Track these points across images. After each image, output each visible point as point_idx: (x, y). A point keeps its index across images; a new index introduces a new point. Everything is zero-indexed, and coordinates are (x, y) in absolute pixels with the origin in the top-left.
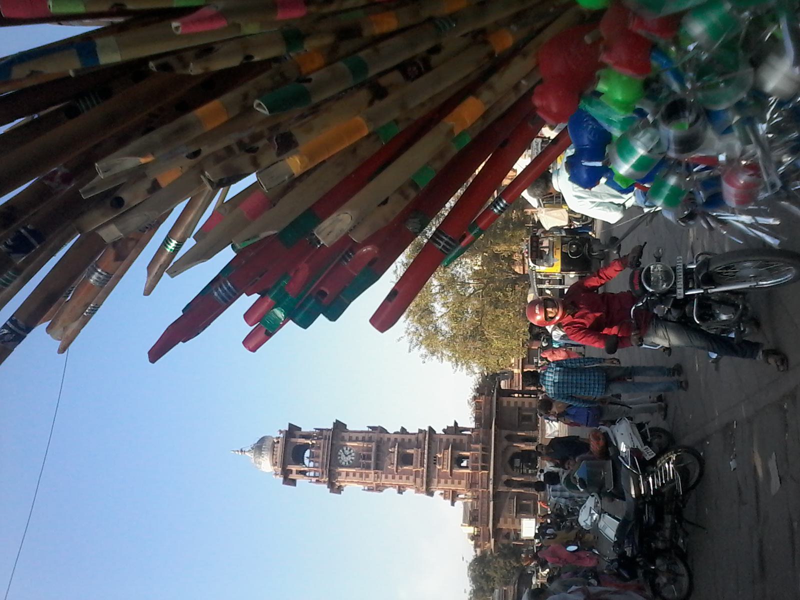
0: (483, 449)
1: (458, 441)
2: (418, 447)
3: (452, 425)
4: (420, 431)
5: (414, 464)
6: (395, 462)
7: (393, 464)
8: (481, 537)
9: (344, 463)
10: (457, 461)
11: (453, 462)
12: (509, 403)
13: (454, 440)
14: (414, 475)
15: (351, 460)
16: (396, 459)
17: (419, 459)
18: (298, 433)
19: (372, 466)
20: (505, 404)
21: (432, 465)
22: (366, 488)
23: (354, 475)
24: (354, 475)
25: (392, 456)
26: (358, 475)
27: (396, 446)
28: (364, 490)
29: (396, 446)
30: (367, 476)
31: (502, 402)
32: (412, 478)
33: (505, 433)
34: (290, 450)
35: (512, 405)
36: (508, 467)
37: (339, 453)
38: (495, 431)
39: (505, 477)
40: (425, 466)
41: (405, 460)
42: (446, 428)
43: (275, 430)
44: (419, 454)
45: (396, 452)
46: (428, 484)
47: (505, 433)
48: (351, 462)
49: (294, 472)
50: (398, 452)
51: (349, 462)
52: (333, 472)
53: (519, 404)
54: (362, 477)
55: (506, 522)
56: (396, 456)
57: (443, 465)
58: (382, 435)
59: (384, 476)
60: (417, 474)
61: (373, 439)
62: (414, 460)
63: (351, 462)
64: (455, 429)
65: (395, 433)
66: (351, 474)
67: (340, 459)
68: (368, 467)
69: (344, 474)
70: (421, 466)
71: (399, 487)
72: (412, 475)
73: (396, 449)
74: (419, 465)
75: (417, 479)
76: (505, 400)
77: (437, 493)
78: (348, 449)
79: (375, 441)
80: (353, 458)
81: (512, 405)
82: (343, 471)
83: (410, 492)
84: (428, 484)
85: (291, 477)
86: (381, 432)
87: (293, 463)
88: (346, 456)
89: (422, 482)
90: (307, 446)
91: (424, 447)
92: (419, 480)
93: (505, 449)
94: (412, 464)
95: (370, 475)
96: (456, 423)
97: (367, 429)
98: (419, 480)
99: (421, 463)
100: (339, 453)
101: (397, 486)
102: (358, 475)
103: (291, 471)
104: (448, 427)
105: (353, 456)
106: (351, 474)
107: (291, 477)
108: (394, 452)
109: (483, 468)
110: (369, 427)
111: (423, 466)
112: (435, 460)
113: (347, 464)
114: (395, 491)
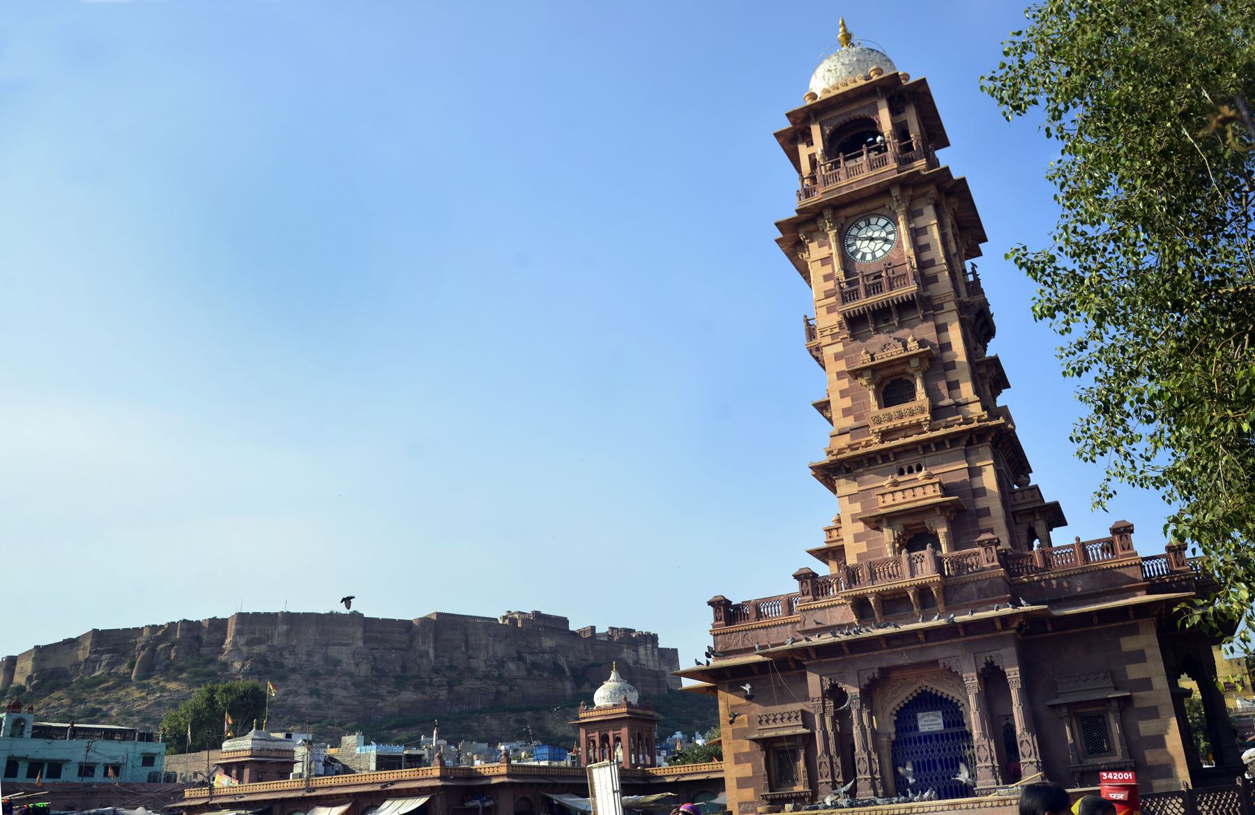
0: (923, 592)
2: (937, 412)
10: (913, 531)
11: (909, 521)
12: (1139, 657)
13: (986, 512)
15: (864, 255)
17: (898, 423)
19: (852, 306)
20: (1129, 644)
21: (894, 465)
24: (827, 278)
31: (1133, 631)
32: (849, 422)
34: (856, 111)
35: (1134, 672)
36: (901, 696)
37: (873, 220)
38: (1005, 620)
41: (891, 385)
44: (914, 420)
49: (811, 150)
53: (1143, 699)
57: (892, 493)
59: (839, 348)
62: (892, 410)
63: (859, 256)
66: (827, 270)
67: (860, 229)
68: (845, 297)
69: (824, 252)
72: (856, 419)
76: (1147, 641)
78: (891, 237)
80: (869, 257)
81: (1134, 672)
92: (845, 440)
98: (845, 440)
100: (873, 220)
105: (874, 257)
106: (827, 270)
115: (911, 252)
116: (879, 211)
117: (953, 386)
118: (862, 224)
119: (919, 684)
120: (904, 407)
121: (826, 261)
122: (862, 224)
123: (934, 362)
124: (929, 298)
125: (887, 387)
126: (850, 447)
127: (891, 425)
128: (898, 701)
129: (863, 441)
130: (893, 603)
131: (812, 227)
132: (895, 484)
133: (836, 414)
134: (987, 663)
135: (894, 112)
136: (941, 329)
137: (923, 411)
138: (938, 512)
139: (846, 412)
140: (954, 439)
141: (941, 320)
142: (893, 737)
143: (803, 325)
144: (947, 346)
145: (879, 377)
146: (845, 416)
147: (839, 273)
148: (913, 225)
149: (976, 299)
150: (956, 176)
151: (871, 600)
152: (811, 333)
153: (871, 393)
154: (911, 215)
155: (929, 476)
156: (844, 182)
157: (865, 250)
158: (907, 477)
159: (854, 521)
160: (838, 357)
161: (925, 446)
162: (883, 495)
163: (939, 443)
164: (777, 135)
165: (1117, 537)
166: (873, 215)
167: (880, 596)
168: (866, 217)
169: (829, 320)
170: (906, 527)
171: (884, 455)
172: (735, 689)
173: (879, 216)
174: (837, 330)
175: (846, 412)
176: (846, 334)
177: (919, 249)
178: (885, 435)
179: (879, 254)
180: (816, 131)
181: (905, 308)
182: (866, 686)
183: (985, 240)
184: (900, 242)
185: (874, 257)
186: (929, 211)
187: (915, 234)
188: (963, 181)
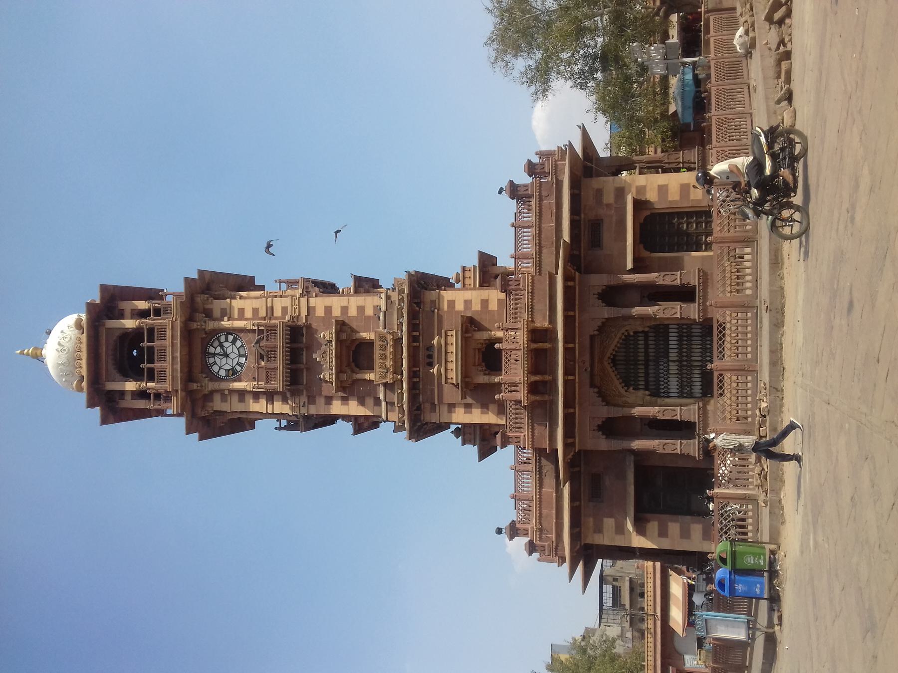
3: (473, 261)
5: (376, 366)
21: (421, 369)
22: (284, 423)
28: (280, 428)
33: (599, 281)
62: (377, 361)
67: (215, 363)
87: (118, 376)
88: (226, 355)
93: (600, 329)
94: (371, 368)
101: (353, 419)
103: (122, 393)
104: (464, 268)
108: (330, 342)
114: (349, 427)
118: (211, 360)
120: (377, 352)
134: (599, 299)
135: (121, 315)
138: (470, 335)
140: (413, 316)
161: (413, 339)
168: (206, 354)
180: (113, 386)
182: (603, 401)
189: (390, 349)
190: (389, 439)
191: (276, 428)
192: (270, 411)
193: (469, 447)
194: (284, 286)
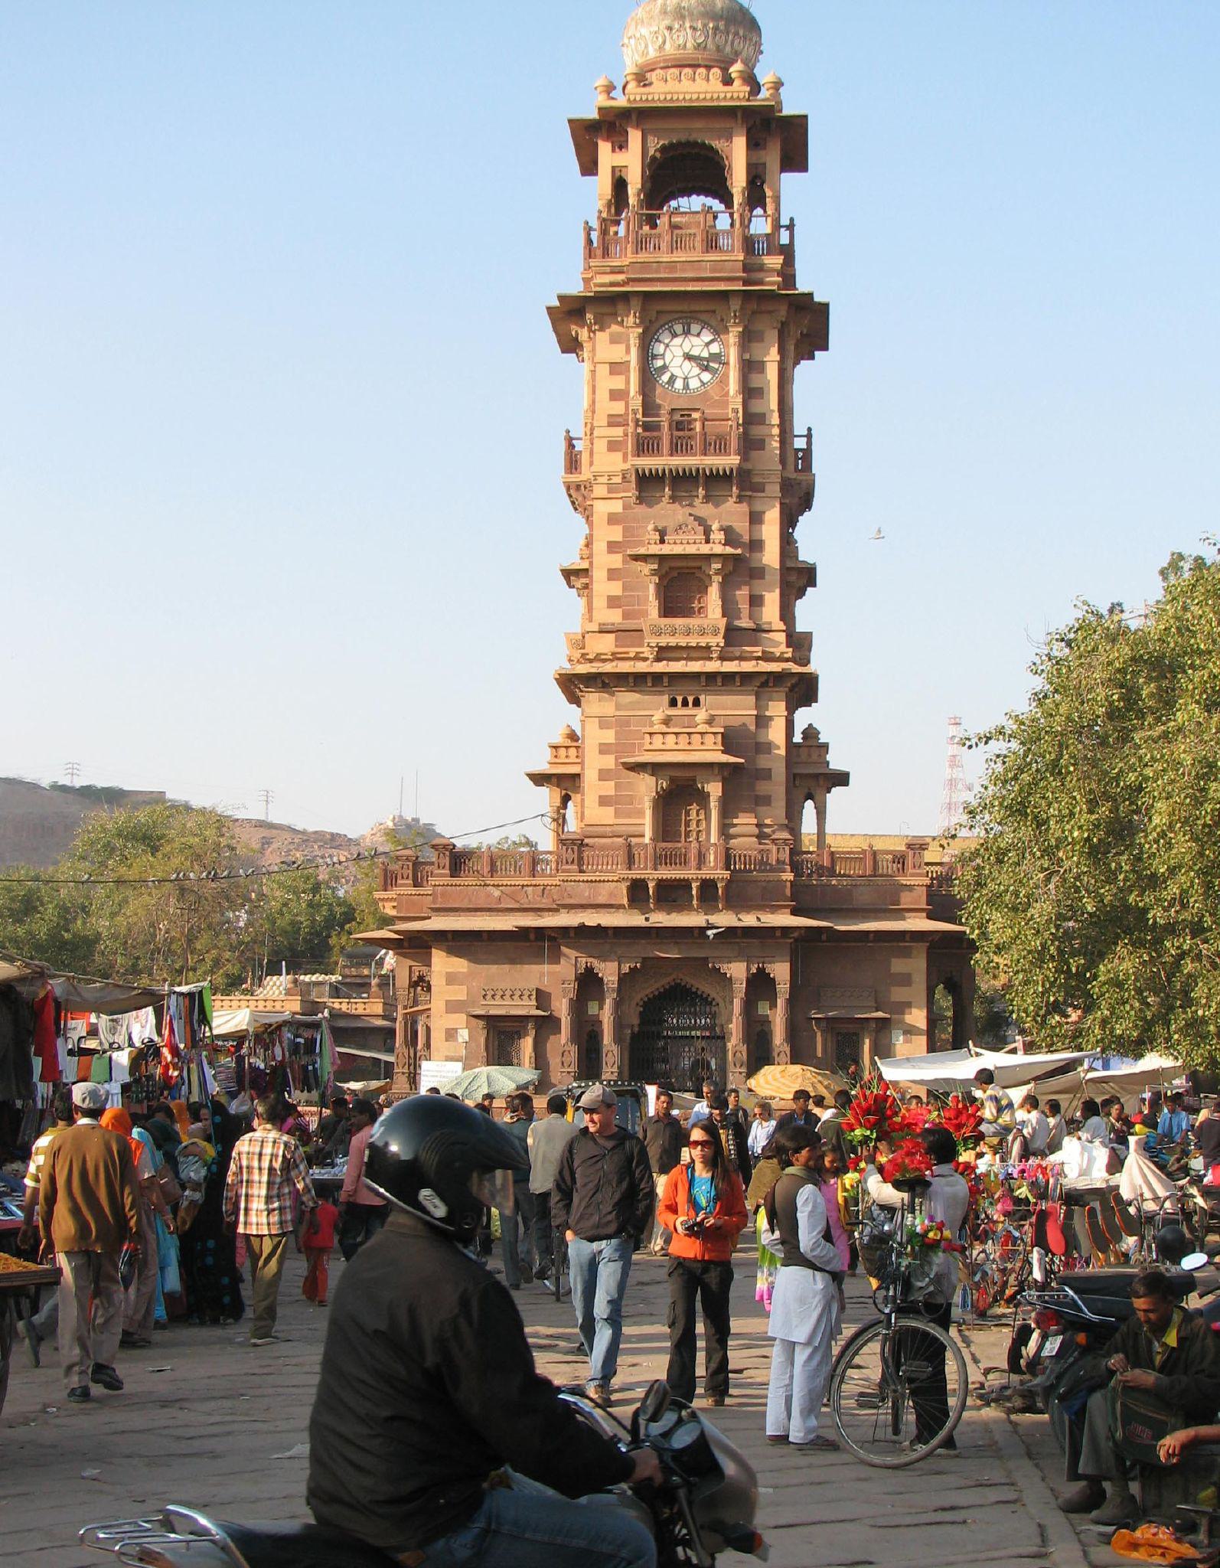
0: (708, 886)
1: (762, 788)
2: (733, 635)
3: (836, 761)
4: (801, 644)
6: (666, 549)
7: (662, 541)
8: (413, 891)
9: (660, 348)
10: (678, 790)
12: (906, 980)
13: (767, 775)
14: (631, 624)
15: (672, 379)
16: (678, 550)
17: (683, 642)
18: (772, 157)
20: (898, 966)
23: (615, 395)
24: (615, 395)
25: (691, 537)
26: (618, 408)
27: (729, 550)
29: (729, 550)
30: (613, 446)
31: (906, 953)
32: (615, 617)
33: (781, 971)
35: (898, 994)
38: (786, 930)
39: (609, 972)
40: (660, 667)
41: (678, 584)
42: (823, 739)
43: (793, 71)
45: (705, 549)
46: (604, 682)
47: (781, 971)
48: (665, 378)
50: (708, 558)
51: (665, 367)
52: (621, 308)
54: (610, 425)
55: (451, 979)
56: (691, 550)
58: (774, 489)
59: (617, 507)
60: (625, 633)
61: (754, 454)
62: (679, 622)
63: (665, 378)
64: (817, 776)
65: (788, 543)
66: (618, 383)
67: (675, 335)
68: (644, 447)
69: (617, 353)
70: (661, 649)
71: (585, 572)
73: (718, 549)
74: (664, 641)
75: (612, 636)
76: (916, 965)
77: (572, 715)
79: (748, 466)
80: (679, 384)
82: (628, 351)
83: (568, 611)
84: (604, 682)
85: (604, 148)
86: (787, 486)
89: (598, 658)
90: (726, 199)
91: (731, 659)
92: (606, 644)
94: (667, 611)
95: (619, 456)
96: (842, 779)
97: (799, 428)
98: (606, 644)
99: (668, 648)
101: (585, 565)
102: (618, 408)
103: (621, 145)
105: (686, 386)
106: (618, 383)
107: (604, 148)
108: (707, 541)
109: (637, 892)
110: (809, 436)
111: (658, 659)
112: (685, 703)
113: (659, 363)
114: (575, 562)
115: (740, 399)
116: (704, 317)
117: (756, 601)
118: (678, 328)
119: (674, 976)
121: (617, 368)
122: (678, 328)
123: (740, 568)
124: (749, 472)
125: (672, 580)
126: (615, 657)
127: (673, 641)
128: (648, 991)
129: (632, 652)
130: (672, 894)
131: (605, 309)
132: (667, 721)
133: (600, 602)
135: (753, 145)
136: (756, 519)
137: (715, 633)
138: (716, 771)
139: (613, 602)
140: (746, 677)
141: (758, 508)
142: (636, 1029)
143: (562, 446)
144: (756, 545)
145: (666, 566)
146: (609, 607)
147: (636, 402)
148: (747, 356)
149: (802, 477)
150: (817, 299)
151: (651, 885)
152: (573, 462)
153: (652, 589)
154: (748, 339)
155: (710, 721)
156: (666, 258)
157: (677, 372)
158: (679, 711)
159: (601, 752)
160: (613, 519)
161: (711, 677)
162: (651, 734)
163: (728, 678)
164: (570, 121)
165: (911, 853)
166: (697, 320)
167: (661, 884)
169: (610, 464)
170: (672, 780)
171: (657, 678)
172: (452, 951)
173: (705, 324)
174: (618, 480)
175: (613, 602)
176: (632, 493)
177: (750, 392)
178: (663, 653)
179: (694, 384)
180: (635, 137)
181: (716, 482)
183: (826, 348)
184: (724, 381)
185: (686, 386)
186: (772, 336)
187: (750, 367)
188: (827, 305)
189: (693, 642)
190: (556, 627)
191: (568, 432)
192: (596, 433)
193: (548, 754)
194: (800, 443)
